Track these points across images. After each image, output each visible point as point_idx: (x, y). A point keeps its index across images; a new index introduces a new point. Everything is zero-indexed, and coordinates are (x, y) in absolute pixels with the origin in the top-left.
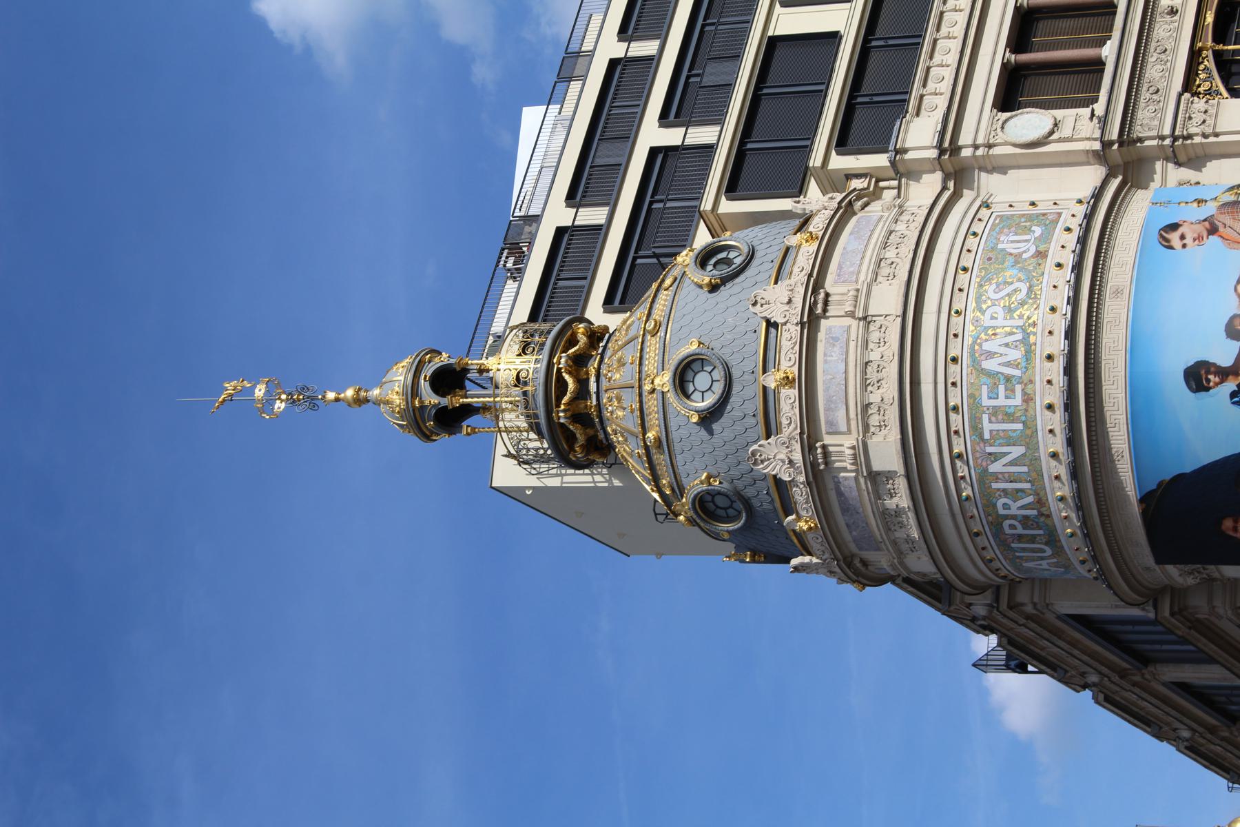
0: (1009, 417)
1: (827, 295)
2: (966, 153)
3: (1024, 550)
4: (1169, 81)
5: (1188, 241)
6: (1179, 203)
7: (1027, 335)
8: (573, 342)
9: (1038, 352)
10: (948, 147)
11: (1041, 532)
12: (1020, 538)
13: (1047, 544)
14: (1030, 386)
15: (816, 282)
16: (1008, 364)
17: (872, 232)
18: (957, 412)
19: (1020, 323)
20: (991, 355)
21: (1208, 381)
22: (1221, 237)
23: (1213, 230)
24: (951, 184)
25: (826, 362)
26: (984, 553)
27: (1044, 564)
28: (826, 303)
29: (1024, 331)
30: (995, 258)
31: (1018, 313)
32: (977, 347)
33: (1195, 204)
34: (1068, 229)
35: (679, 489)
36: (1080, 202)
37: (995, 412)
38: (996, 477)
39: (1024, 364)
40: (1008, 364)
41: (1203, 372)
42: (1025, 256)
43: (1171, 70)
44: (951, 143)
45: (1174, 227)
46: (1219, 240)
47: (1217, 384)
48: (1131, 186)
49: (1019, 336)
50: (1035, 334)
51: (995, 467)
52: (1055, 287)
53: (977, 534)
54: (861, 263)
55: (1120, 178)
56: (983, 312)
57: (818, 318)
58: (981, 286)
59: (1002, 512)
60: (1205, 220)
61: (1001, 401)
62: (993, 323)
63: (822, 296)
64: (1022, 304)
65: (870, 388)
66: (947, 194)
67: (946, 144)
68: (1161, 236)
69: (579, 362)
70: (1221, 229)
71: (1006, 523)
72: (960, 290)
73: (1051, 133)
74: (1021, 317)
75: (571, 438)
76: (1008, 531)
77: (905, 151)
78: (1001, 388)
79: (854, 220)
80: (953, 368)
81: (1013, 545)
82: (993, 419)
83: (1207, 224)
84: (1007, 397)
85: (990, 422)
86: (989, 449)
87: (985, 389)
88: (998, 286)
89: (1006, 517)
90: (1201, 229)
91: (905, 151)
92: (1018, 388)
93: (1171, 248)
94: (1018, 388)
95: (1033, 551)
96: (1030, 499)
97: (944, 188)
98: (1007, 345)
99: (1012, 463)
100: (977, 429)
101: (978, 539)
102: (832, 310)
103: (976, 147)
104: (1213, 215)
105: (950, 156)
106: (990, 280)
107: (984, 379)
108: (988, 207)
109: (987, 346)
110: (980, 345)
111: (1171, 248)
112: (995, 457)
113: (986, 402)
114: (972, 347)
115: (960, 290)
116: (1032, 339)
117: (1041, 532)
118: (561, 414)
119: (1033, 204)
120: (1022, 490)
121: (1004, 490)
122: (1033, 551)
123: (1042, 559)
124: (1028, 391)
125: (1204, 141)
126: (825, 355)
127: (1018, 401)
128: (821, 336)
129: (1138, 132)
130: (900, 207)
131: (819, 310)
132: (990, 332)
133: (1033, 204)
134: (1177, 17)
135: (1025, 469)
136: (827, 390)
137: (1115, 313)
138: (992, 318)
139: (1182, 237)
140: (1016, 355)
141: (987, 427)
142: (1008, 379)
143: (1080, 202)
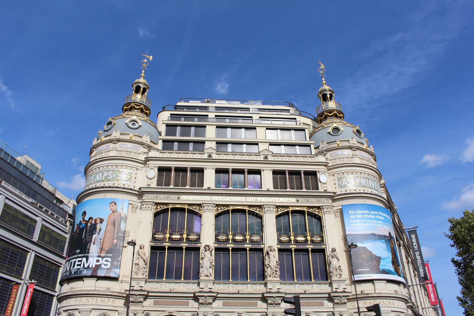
0: (90, 181)
1: (116, 143)
4: (158, 200)
5: (111, 207)
6: (122, 205)
15: (119, 140)
17: (133, 149)
19: (103, 179)
22: (112, 214)
23: (113, 212)
24: (144, 162)
28: (115, 143)
40: (97, 179)
43: (162, 200)
44: (149, 159)
45: (115, 204)
46: (111, 213)
52: (109, 184)
55: (138, 193)
56: (107, 172)
57: (112, 143)
60: (116, 210)
61: (92, 179)
63: (116, 142)
67: (148, 159)
68: (113, 202)
70: (114, 213)
72: (112, 167)
73: (149, 178)
77: (150, 152)
79: (141, 146)
88: (112, 173)
90: (114, 210)
91: (150, 152)
92: (93, 181)
93: (110, 204)
94: (93, 181)
97: (143, 161)
98: (100, 177)
103: (148, 165)
104: (118, 211)
105: (147, 160)
108: (137, 169)
111: (110, 204)
119: (136, 178)
127: (92, 182)
128: (109, 144)
129: (146, 195)
130: (140, 154)
131: (114, 142)
133: (136, 178)
134: (177, 199)
139: (112, 206)
140: (98, 180)
141: (90, 178)
142: (95, 179)
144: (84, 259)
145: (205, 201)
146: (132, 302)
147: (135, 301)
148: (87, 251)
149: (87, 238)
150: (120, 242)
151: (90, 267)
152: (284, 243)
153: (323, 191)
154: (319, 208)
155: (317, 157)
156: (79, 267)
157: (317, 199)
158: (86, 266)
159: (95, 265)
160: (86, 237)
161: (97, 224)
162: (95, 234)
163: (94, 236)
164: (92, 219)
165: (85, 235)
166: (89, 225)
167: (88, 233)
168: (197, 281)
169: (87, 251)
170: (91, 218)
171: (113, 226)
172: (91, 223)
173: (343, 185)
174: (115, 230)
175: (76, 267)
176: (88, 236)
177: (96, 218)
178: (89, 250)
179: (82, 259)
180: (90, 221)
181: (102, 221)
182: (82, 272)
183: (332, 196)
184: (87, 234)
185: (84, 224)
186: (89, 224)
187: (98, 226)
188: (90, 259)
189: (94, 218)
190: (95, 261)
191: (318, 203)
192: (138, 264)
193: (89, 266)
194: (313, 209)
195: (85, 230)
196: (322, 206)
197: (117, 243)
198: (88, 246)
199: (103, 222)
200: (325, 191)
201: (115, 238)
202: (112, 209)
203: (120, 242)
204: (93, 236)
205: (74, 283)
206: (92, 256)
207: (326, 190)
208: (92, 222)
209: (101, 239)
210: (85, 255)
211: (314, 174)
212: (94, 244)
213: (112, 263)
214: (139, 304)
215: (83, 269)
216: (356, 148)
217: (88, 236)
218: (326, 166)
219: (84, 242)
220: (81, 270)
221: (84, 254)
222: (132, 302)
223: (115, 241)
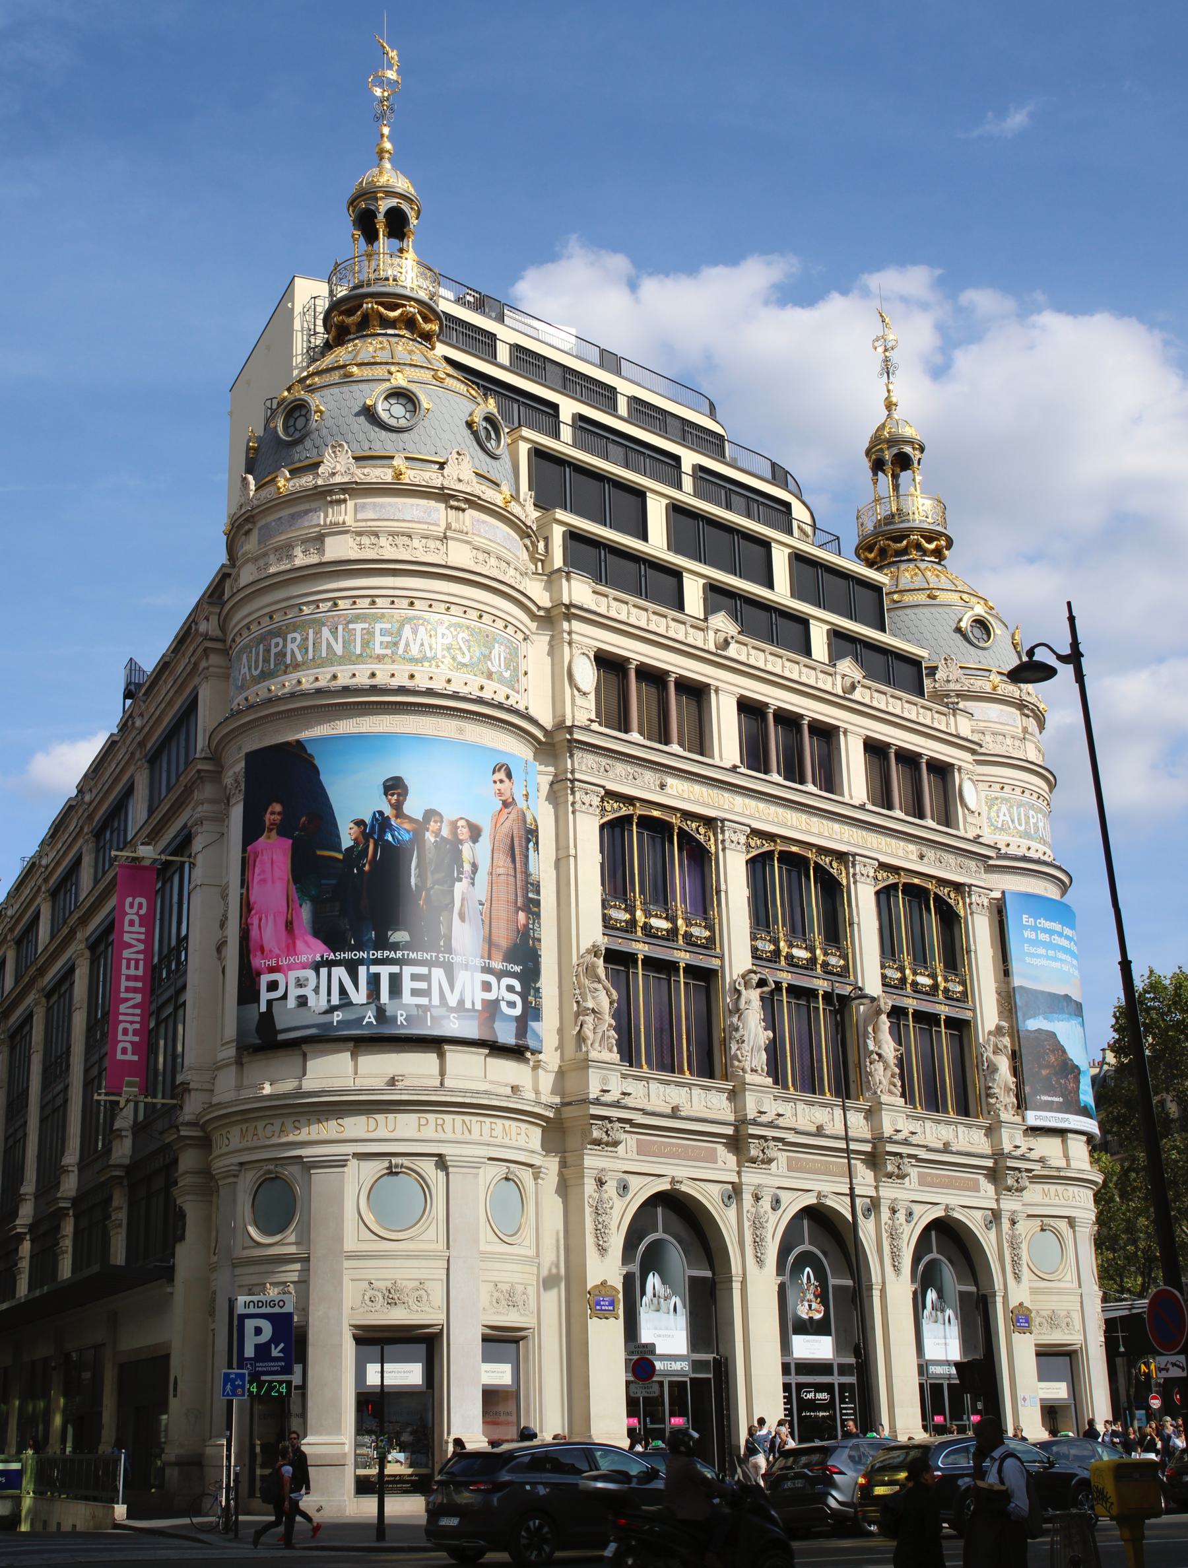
0: (366, 644)
1: (463, 510)
2: (566, 625)
3: (257, 654)
5: (499, 785)
7: (430, 660)
8: (426, 319)
9: (416, 668)
10: (570, 612)
11: (272, 667)
12: (268, 651)
13: (262, 671)
14: (390, 660)
15: (474, 502)
16: (407, 645)
17: (509, 550)
18: (370, 604)
19: (439, 656)
20: (415, 632)
21: (392, 795)
23: (506, 804)
24: (542, 613)
25: (413, 505)
26: (256, 623)
27: (246, 669)
28: (458, 509)
29: (433, 658)
30: (488, 641)
31: (447, 654)
32: (421, 621)
33: (525, 793)
34: (508, 697)
35: (311, 389)
36: (527, 709)
37: (370, 633)
38: (318, 633)
39: (407, 656)
40: (407, 645)
41: (399, 791)
42: (489, 663)
43: (621, 782)
44: (573, 614)
45: (509, 775)
46: (499, 809)
47: (389, 801)
48: (536, 748)
49: (429, 654)
50: (430, 666)
51: (326, 632)
53: (271, 618)
54: (487, 539)
55: (544, 740)
56: (447, 628)
58: (468, 628)
59: (289, 637)
61: (378, 638)
62: (439, 635)
63: (463, 506)
64: (454, 658)
65: (391, 538)
66: (534, 609)
67: (573, 610)
68: (503, 765)
69: (409, 323)
70: (506, 810)
71: (280, 640)
72: (465, 612)
73: (579, 690)
74: (444, 657)
75: (350, 312)
76: (274, 641)
77: (568, 580)
78: (389, 639)
79: (518, 539)
80: (406, 602)
81: (261, 646)
82: (365, 632)
83: (511, 800)
84: (381, 643)
85: (362, 629)
86: (340, 628)
87: (388, 626)
89: (285, 640)
90: (507, 796)
91: (568, 580)
92: (389, 652)
93: (494, 772)
94: (389, 652)
95: (257, 661)
96: (299, 658)
97: (539, 608)
98: (422, 645)
99: (329, 644)
100: (357, 619)
101: (267, 619)
102: (452, 513)
103: (570, 633)
105: (564, 613)
106: (472, 635)
107: (396, 625)
108: (525, 639)
109: (422, 629)
110: (422, 624)
111: (494, 772)
112: (334, 632)
113: (378, 627)
114: (420, 618)
115: (465, 612)
116: (426, 664)
117: (272, 667)
118: (370, 305)
120: (307, 652)
121: (307, 639)
122: (257, 661)
123: (250, 669)
124: (386, 659)
125: (570, 803)
126: (418, 505)
127: (378, 650)
128: (432, 503)
129: (578, 754)
130: (526, 573)
131: (453, 503)
132: (433, 633)
133: (526, 673)
134: (658, 789)
135: (324, 655)
136: (390, 505)
137: (445, 727)
138: (443, 635)
139: (501, 781)
140: (415, 651)
141: (359, 627)
142: (396, 644)
143: (527, 709)
144: (438, 974)
145: (725, 810)
146: (597, 1142)
147: (605, 1138)
148: (442, 943)
149: (432, 892)
150: (533, 924)
151: (468, 1005)
152: (797, 966)
153: (970, 836)
154: (958, 887)
155: (954, 715)
156: (423, 1001)
157: (960, 859)
158: (452, 1001)
159: (483, 1001)
160: (429, 885)
161: (461, 842)
162: (460, 880)
163: (460, 888)
164: (437, 818)
165: (421, 876)
166: (433, 840)
167: (433, 873)
168: (729, 1086)
169: (442, 943)
170: (430, 814)
171: (509, 860)
172: (437, 833)
173: (1000, 826)
174: (519, 876)
175: (407, 998)
176: (435, 883)
177: (454, 818)
178: (449, 938)
179: (430, 971)
180: (433, 826)
181: (475, 833)
182: (444, 1022)
183: (989, 858)
184: (429, 874)
185: (408, 831)
186: (430, 837)
187: (466, 849)
188: (462, 977)
189: (449, 814)
190: (478, 986)
191: (961, 874)
192: (593, 1011)
193: (461, 1002)
194: (944, 887)
195: (419, 857)
196: (970, 886)
197: (526, 926)
198: (440, 922)
199: (480, 839)
200: (976, 840)
201: (519, 904)
202: (500, 794)
203: (533, 924)
204: (453, 886)
205: (393, 1056)
206: (466, 966)
207: (979, 836)
208: (440, 829)
209: (483, 905)
210: (437, 957)
211: (942, 770)
212: (462, 918)
213: (524, 996)
214: (609, 1149)
215: (442, 1011)
216: (1032, 710)
217: (435, 883)
218: (974, 752)
219: (421, 902)
220: (435, 1012)
221: (434, 954)
222: (597, 1142)
223: (522, 916)
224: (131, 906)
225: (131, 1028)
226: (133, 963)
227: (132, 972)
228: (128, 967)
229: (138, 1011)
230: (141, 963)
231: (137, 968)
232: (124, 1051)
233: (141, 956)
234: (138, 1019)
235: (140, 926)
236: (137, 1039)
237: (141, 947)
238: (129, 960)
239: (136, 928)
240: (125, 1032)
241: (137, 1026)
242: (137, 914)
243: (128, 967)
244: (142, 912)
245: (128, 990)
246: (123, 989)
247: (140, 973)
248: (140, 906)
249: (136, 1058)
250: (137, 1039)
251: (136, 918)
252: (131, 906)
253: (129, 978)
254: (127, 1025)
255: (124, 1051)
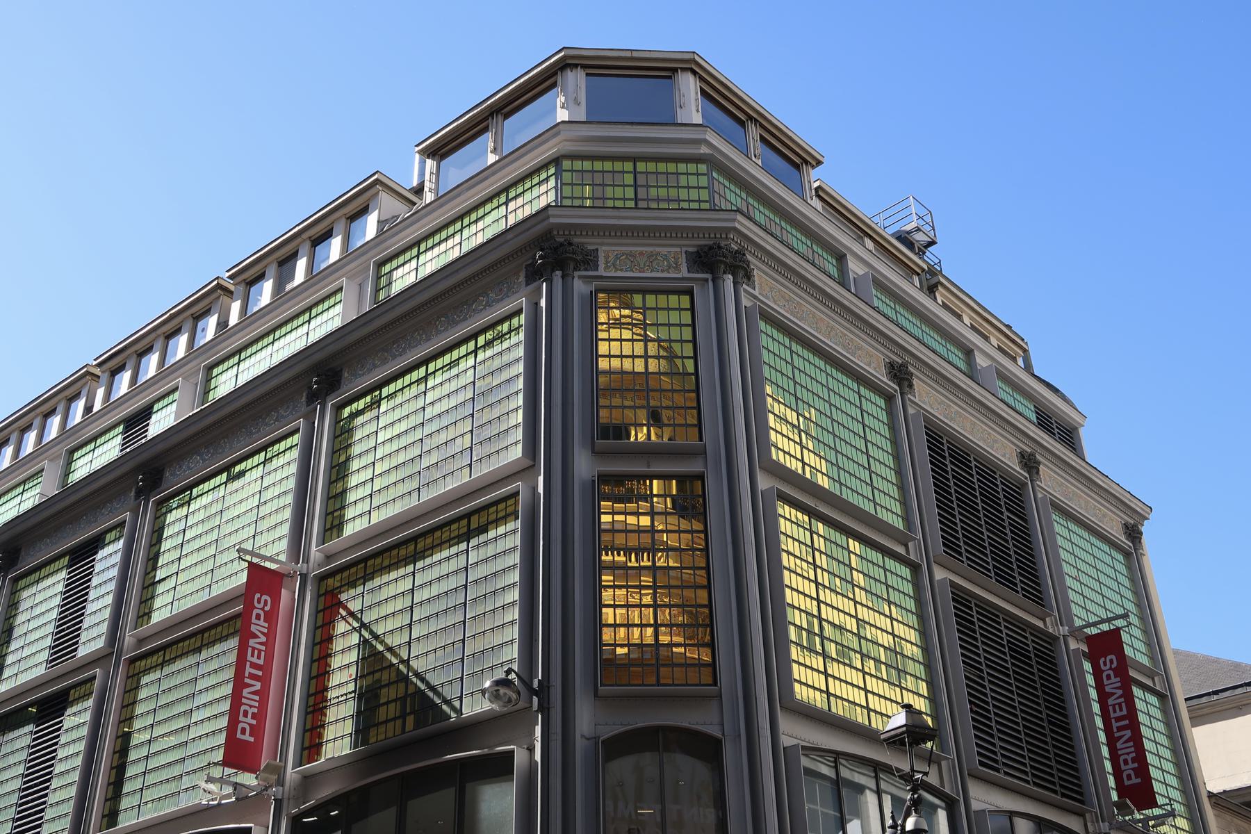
159: (1115, 677)
224: (1105, 664)
225: (1129, 758)
226: (1117, 707)
227: (1119, 714)
228: (1115, 711)
229: (1131, 744)
230: (1123, 705)
231: (1121, 710)
232: (1129, 777)
233: (1122, 700)
234: (1133, 749)
235: (265, 621)
236: (1136, 765)
237: (1120, 692)
238: (1114, 706)
239: (1113, 679)
240: (1126, 762)
241: (1134, 755)
242: (1111, 669)
243: (1115, 711)
244: (1114, 665)
245: (1120, 729)
246: (1115, 730)
247: (1125, 712)
248: (1111, 661)
249: (1139, 780)
250: (1136, 765)
251: (1111, 673)
252: (1105, 664)
253: (1118, 719)
254: (1126, 756)
255: (1129, 777)
